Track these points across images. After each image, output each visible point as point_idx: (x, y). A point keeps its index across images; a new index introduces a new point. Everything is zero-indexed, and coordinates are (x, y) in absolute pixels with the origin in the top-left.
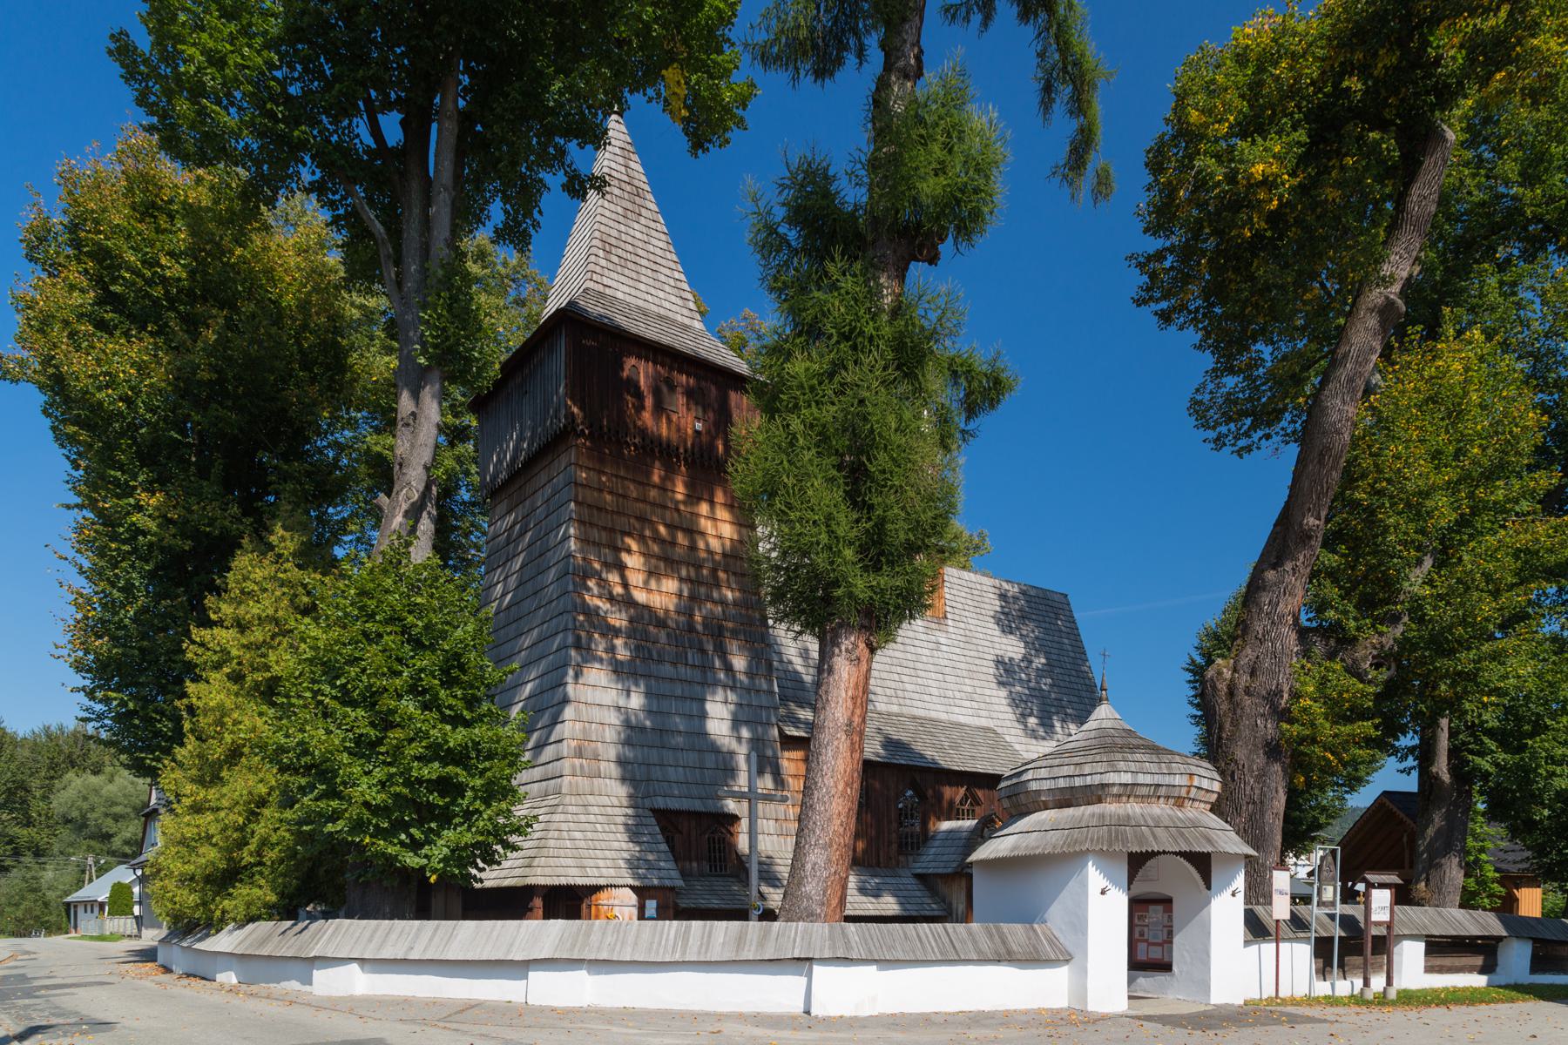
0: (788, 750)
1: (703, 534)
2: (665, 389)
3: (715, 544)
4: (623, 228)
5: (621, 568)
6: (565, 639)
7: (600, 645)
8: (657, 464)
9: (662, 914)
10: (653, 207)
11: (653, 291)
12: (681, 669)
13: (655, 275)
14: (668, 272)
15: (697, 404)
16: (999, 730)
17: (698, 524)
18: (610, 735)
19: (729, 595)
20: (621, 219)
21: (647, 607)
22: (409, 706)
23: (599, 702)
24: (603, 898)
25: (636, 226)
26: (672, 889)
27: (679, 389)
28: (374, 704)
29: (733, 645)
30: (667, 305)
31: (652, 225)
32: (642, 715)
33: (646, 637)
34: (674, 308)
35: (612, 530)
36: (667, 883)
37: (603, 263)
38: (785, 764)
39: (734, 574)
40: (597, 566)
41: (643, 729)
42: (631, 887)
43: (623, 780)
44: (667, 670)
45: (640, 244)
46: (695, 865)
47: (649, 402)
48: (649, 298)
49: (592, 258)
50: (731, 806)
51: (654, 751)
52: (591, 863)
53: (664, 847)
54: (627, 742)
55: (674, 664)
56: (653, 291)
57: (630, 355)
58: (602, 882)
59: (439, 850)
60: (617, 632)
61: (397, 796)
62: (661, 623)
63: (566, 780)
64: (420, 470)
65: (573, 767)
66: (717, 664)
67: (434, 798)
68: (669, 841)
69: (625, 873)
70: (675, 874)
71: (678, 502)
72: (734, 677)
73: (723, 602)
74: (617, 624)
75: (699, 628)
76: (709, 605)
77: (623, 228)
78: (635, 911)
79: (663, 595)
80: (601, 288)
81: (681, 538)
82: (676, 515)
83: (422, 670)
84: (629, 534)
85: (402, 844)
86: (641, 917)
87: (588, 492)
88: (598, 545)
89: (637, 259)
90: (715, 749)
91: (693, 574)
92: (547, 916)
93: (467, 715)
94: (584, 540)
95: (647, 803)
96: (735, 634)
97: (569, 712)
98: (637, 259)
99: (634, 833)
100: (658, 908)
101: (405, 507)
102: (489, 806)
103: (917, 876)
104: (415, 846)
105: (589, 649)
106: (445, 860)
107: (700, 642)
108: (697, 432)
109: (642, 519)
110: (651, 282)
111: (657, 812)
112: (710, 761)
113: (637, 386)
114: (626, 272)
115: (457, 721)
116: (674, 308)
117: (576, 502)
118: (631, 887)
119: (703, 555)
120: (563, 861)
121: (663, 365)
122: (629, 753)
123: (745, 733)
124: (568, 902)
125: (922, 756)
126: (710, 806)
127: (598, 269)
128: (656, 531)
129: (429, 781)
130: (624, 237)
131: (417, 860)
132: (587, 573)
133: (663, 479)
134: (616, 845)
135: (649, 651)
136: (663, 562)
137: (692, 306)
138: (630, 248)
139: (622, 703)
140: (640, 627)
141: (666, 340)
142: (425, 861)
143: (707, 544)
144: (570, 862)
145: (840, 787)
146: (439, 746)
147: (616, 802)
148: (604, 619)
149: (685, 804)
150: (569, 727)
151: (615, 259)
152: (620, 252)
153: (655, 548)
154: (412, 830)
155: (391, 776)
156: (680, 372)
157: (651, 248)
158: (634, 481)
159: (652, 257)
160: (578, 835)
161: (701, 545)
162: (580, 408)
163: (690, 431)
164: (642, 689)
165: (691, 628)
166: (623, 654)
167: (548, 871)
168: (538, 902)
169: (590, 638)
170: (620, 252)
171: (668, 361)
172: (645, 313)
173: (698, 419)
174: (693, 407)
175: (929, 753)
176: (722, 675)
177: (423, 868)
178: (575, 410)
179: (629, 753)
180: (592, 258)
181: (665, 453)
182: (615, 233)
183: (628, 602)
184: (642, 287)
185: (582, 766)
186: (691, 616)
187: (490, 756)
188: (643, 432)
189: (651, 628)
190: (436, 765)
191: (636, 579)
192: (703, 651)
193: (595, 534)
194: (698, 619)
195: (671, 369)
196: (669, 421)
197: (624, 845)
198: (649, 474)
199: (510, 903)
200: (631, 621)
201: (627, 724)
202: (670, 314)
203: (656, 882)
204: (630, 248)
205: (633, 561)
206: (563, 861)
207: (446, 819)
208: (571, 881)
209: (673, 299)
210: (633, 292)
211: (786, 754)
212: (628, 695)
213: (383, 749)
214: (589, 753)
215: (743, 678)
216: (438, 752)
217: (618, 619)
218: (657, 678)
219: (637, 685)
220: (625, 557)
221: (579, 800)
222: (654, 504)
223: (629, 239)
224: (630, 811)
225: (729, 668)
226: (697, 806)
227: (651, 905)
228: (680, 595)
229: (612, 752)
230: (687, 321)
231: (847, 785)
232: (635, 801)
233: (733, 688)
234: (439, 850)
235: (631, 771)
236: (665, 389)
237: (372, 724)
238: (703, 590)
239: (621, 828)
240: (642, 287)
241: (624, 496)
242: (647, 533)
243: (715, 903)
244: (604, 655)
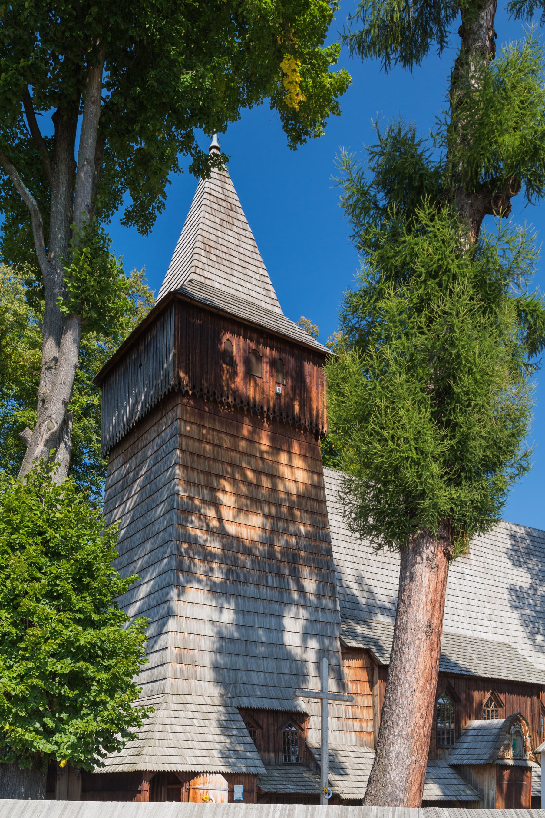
0: (348, 659)
1: (282, 478)
2: (253, 360)
3: (292, 488)
4: (220, 234)
5: (216, 504)
6: (169, 563)
7: (199, 567)
9: (247, 798)
10: (244, 219)
11: (243, 283)
12: (263, 590)
13: (244, 271)
14: (255, 269)
15: (278, 372)
16: (514, 645)
17: (278, 470)
18: (207, 644)
19: (302, 529)
20: (218, 227)
21: (237, 538)
22: (46, 609)
23: (199, 616)
24: (199, 782)
25: (230, 233)
26: (256, 775)
27: (265, 360)
28: (16, 607)
29: (305, 571)
30: (254, 294)
31: (242, 232)
32: (233, 628)
33: (235, 562)
34: (259, 296)
35: (208, 474)
36: (253, 770)
37: (204, 260)
38: (346, 670)
39: (306, 511)
40: (197, 503)
41: (232, 640)
42: (223, 774)
43: (216, 682)
44: (252, 590)
45: (233, 247)
46: (272, 755)
47: (241, 369)
48: (240, 288)
49: (196, 257)
50: (303, 705)
51: (240, 659)
52: (189, 752)
53: (249, 739)
54: (220, 651)
55: (257, 585)
56: (243, 283)
57: (226, 330)
58: (199, 769)
59: (67, 739)
60: (213, 556)
61: (34, 687)
62: (248, 552)
63: (169, 682)
64: (60, 405)
65: (175, 671)
66: (293, 586)
67: (66, 691)
68: (252, 734)
69: (218, 761)
70: (258, 763)
71: (261, 452)
72: (305, 597)
73: (297, 535)
74: (213, 550)
75: (279, 555)
76: (286, 537)
77: (220, 234)
78: (226, 794)
79: (250, 527)
80: (202, 279)
81: (266, 482)
82: (260, 463)
83: (57, 577)
84: (223, 477)
85: (37, 731)
86: (231, 800)
87: (191, 442)
88: (197, 485)
89: (231, 258)
90: (290, 658)
91: (273, 510)
92: (152, 799)
93: (95, 617)
94: (188, 482)
95: (235, 702)
96: (307, 562)
97: (171, 624)
98: (231, 258)
99: (225, 728)
100: (244, 792)
101: (46, 436)
102: (112, 697)
103: (455, 767)
104: (48, 733)
105: (189, 571)
106: (73, 746)
107: (278, 568)
108: (278, 395)
110: (241, 276)
111: (243, 710)
112: (285, 667)
113: (232, 358)
114: (222, 268)
115: (87, 623)
116: (259, 296)
117: (182, 451)
118: (223, 774)
119: (283, 496)
120: (167, 751)
121: (251, 339)
122: (221, 660)
123: (313, 644)
124: (169, 785)
125: (457, 665)
126: (286, 706)
127: (200, 265)
128: (245, 475)
129: (63, 675)
130: (220, 241)
131: (49, 746)
132: (187, 511)
134: (210, 738)
135: (238, 575)
136: (251, 501)
137: (273, 295)
138: (225, 249)
139: (215, 617)
140: (230, 554)
141: (255, 319)
142: (55, 747)
143: (285, 487)
144: (172, 751)
145: (421, 683)
146: (71, 643)
147: (209, 702)
148: (203, 546)
149: (265, 704)
150: (174, 635)
151: (214, 258)
152: (217, 252)
153: (244, 489)
154: (46, 720)
155: (29, 670)
156: (265, 345)
157: (242, 250)
158: (227, 434)
159: (242, 257)
160: (178, 729)
161: (281, 487)
162: (186, 373)
163: (272, 394)
164: (233, 606)
165: (271, 555)
166: (218, 576)
167: (154, 759)
168: (145, 786)
169: (192, 559)
170: (217, 252)
171: (255, 336)
172: (237, 299)
173: (278, 384)
174: (275, 374)
175: (462, 663)
176: (295, 596)
177: (53, 754)
178: (182, 375)
179: (221, 660)
180: (196, 257)
182: (213, 238)
183: (222, 533)
184: (234, 279)
185: (181, 670)
186: (272, 545)
187: (113, 654)
188: (235, 393)
189: (239, 555)
190: (68, 660)
191: (227, 514)
192: (280, 575)
193: (195, 477)
194: (278, 549)
195: (258, 343)
196: (256, 385)
197: (217, 738)
198: (239, 428)
199: (123, 787)
200: (223, 550)
201: (221, 637)
202: (256, 302)
203: (244, 770)
204: (225, 249)
205: (227, 499)
206: (167, 751)
207: (75, 712)
208: (174, 768)
209: (259, 290)
210: (227, 283)
211: (347, 663)
212: (221, 611)
213: (22, 645)
214: (187, 660)
215: (312, 598)
216: (70, 649)
217: (215, 547)
218: (243, 597)
219: (229, 603)
220: (220, 495)
221: (180, 699)
222: (242, 453)
223: (225, 243)
224: (221, 709)
225: (301, 590)
226: (276, 705)
227: (239, 789)
228: (264, 529)
229: (207, 659)
230: (269, 307)
231: (426, 681)
232: (226, 700)
233: (304, 606)
234: (67, 739)
235: (225, 677)
236: (253, 360)
237: (14, 624)
238: (280, 524)
239: (214, 723)
240: (234, 279)
241: (220, 446)
242: (238, 476)
243: (291, 788)
244: (204, 578)
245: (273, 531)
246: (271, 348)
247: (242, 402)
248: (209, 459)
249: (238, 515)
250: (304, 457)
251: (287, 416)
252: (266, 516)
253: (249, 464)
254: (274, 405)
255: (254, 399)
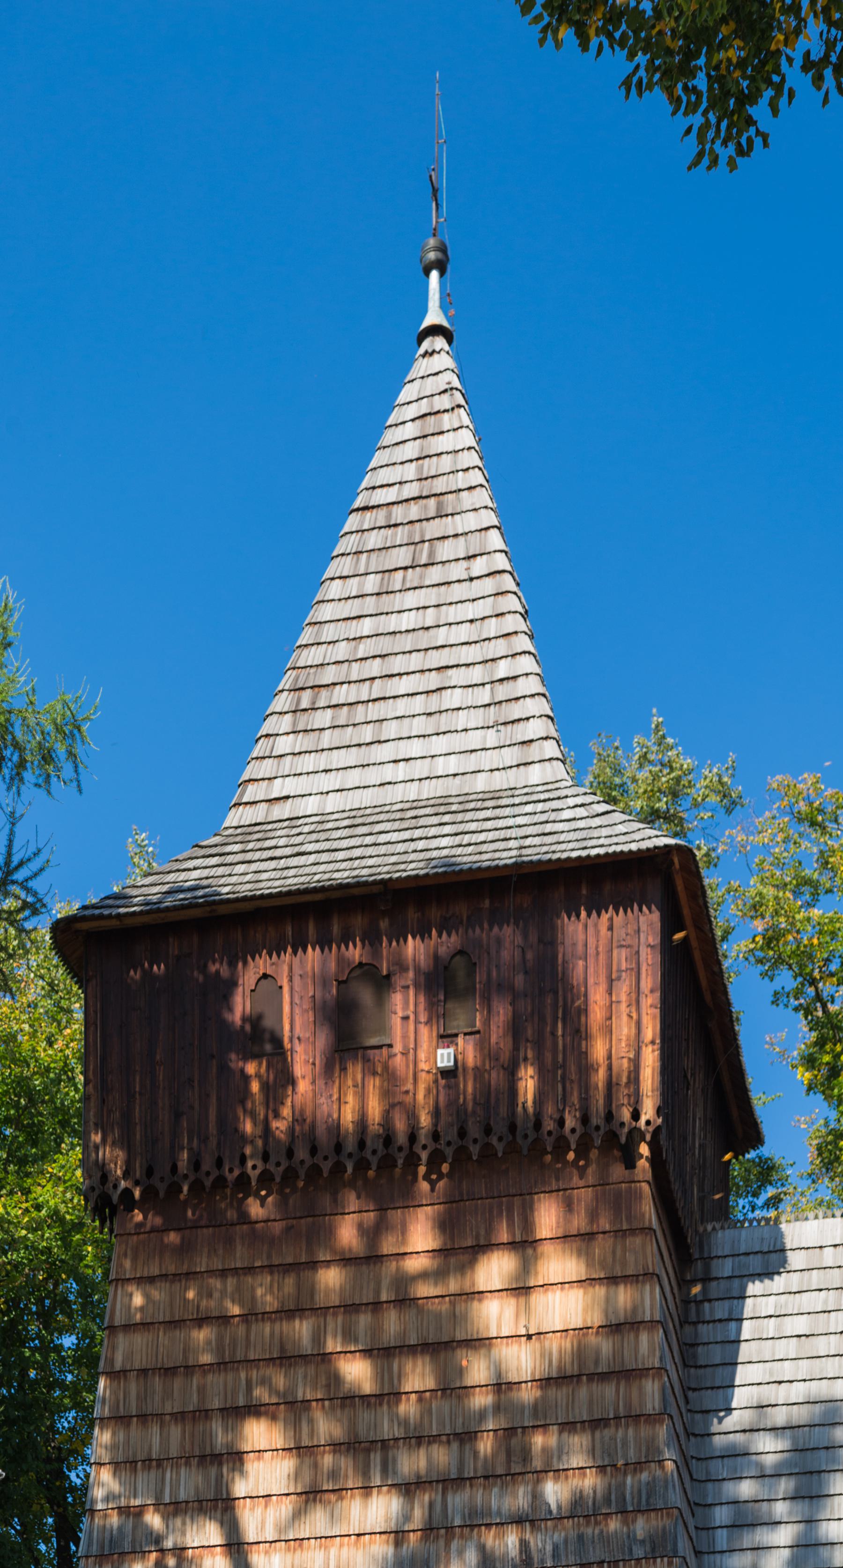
1: (479, 1343)
8: (352, 1201)
39: (568, 1426)
81: (418, 1377)
109: (287, 1358)
119: (481, 1400)
133: (372, 1234)
153: (326, 1427)
161: (478, 1371)
181: (378, 1165)
193: (154, 1439)
195: (372, 939)
228: (398, 1536)
245: (429, 1530)
246: (423, 932)
247: (314, 1151)
248: (205, 1369)
249: (298, 1515)
250: (578, 1240)
251: (488, 1131)
252: (408, 1489)
253: (349, 1335)
254: (436, 1113)
255: (362, 1123)
